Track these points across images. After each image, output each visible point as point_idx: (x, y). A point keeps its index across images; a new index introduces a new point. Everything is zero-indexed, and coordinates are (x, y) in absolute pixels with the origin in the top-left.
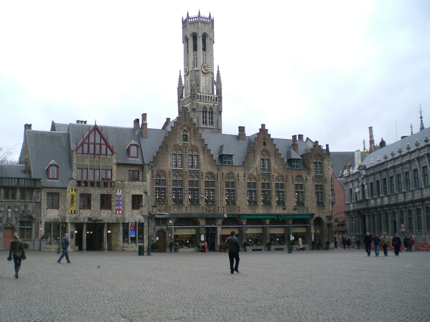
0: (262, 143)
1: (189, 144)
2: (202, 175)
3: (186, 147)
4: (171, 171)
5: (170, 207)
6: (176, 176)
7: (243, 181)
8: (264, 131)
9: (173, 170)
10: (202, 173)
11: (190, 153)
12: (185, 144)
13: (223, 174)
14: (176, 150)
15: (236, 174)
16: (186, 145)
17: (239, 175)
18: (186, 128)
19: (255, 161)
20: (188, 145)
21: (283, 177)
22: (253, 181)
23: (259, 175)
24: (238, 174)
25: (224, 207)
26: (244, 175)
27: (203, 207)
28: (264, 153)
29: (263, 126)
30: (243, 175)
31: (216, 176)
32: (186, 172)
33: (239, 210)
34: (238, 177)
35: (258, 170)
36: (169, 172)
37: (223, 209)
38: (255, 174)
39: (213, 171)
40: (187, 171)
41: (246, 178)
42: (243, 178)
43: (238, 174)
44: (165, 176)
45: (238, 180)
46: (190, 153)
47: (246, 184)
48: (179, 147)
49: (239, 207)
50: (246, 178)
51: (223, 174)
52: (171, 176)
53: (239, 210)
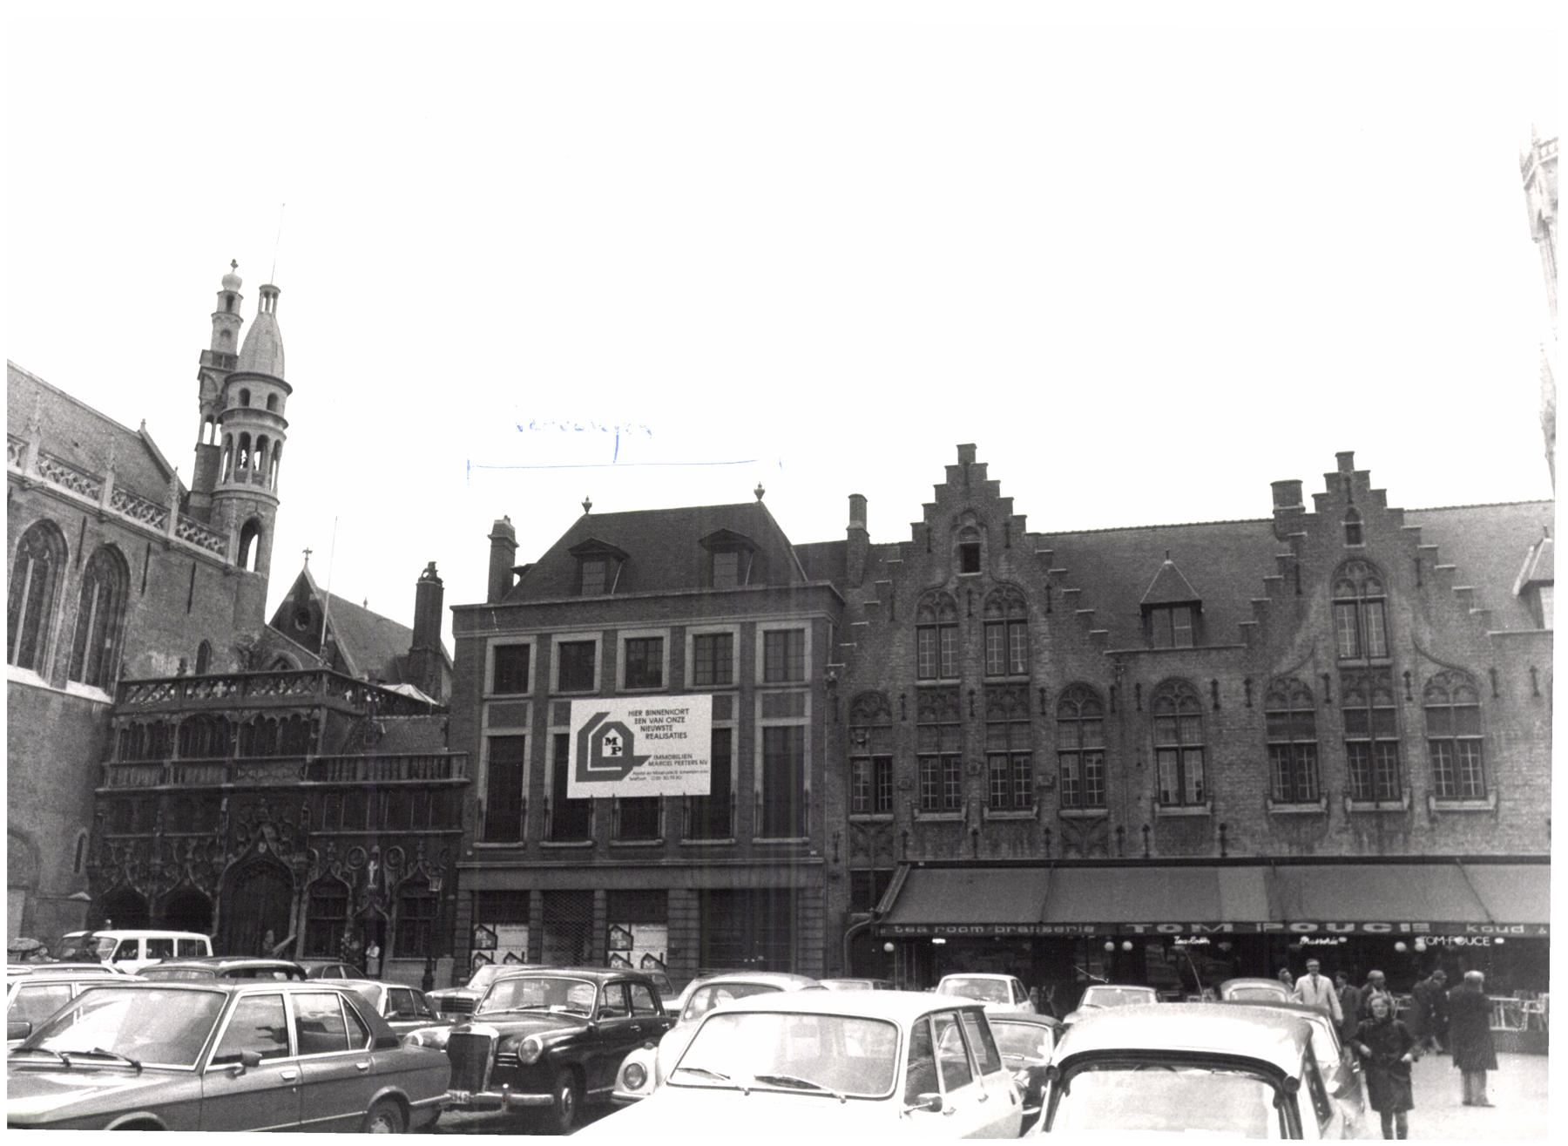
0: (1341, 533)
1: (986, 579)
2: (1043, 701)
3: (970, 592)
4: (910, 694)
5: (905, 834)
6: (933, 711)
7: (1244, 710)
8: (1348, 480)
9: (920, 688)
10: (1042, 691)
11: (994, 614)
12: (963, 581)
13: (1138, 687)
14: (932, 612)
15: (1203, 683)
16: (970, 585)
17: (1221, 689)
18: (971, 522)
19: (1300, 614)
20: (981, 586)
21: (1471, 678)
22: (1301, 705)
23: (1326, 677)
24: (1215, 683)
25: (1146, 829)
26: (1248, 682)
27: (1047, 831)
28: (1357, 576)
29: (1345, 458)
30: (1238, 685)
31: (1107, 697)
32: (972, 693)
33: (1223, 840)
34: (1215, 694)
35: (1321, 655)
36: (903, 696)
37: (1141, 834)
38: (1307, 675)
39: (1091, 680)
40: (977, 688)
41: (1258, 698)
42: (1243, 699)
43: (1215, 683)
44: (889, 714)
45: (1217, 707)
46: (994, 614)
47: (1260, 722)
48: (946, 599)
49: (1223, 827)
50: (1258, 698)
51: (1138, 687)
52: (912, 711)
53: (1223, 840)
